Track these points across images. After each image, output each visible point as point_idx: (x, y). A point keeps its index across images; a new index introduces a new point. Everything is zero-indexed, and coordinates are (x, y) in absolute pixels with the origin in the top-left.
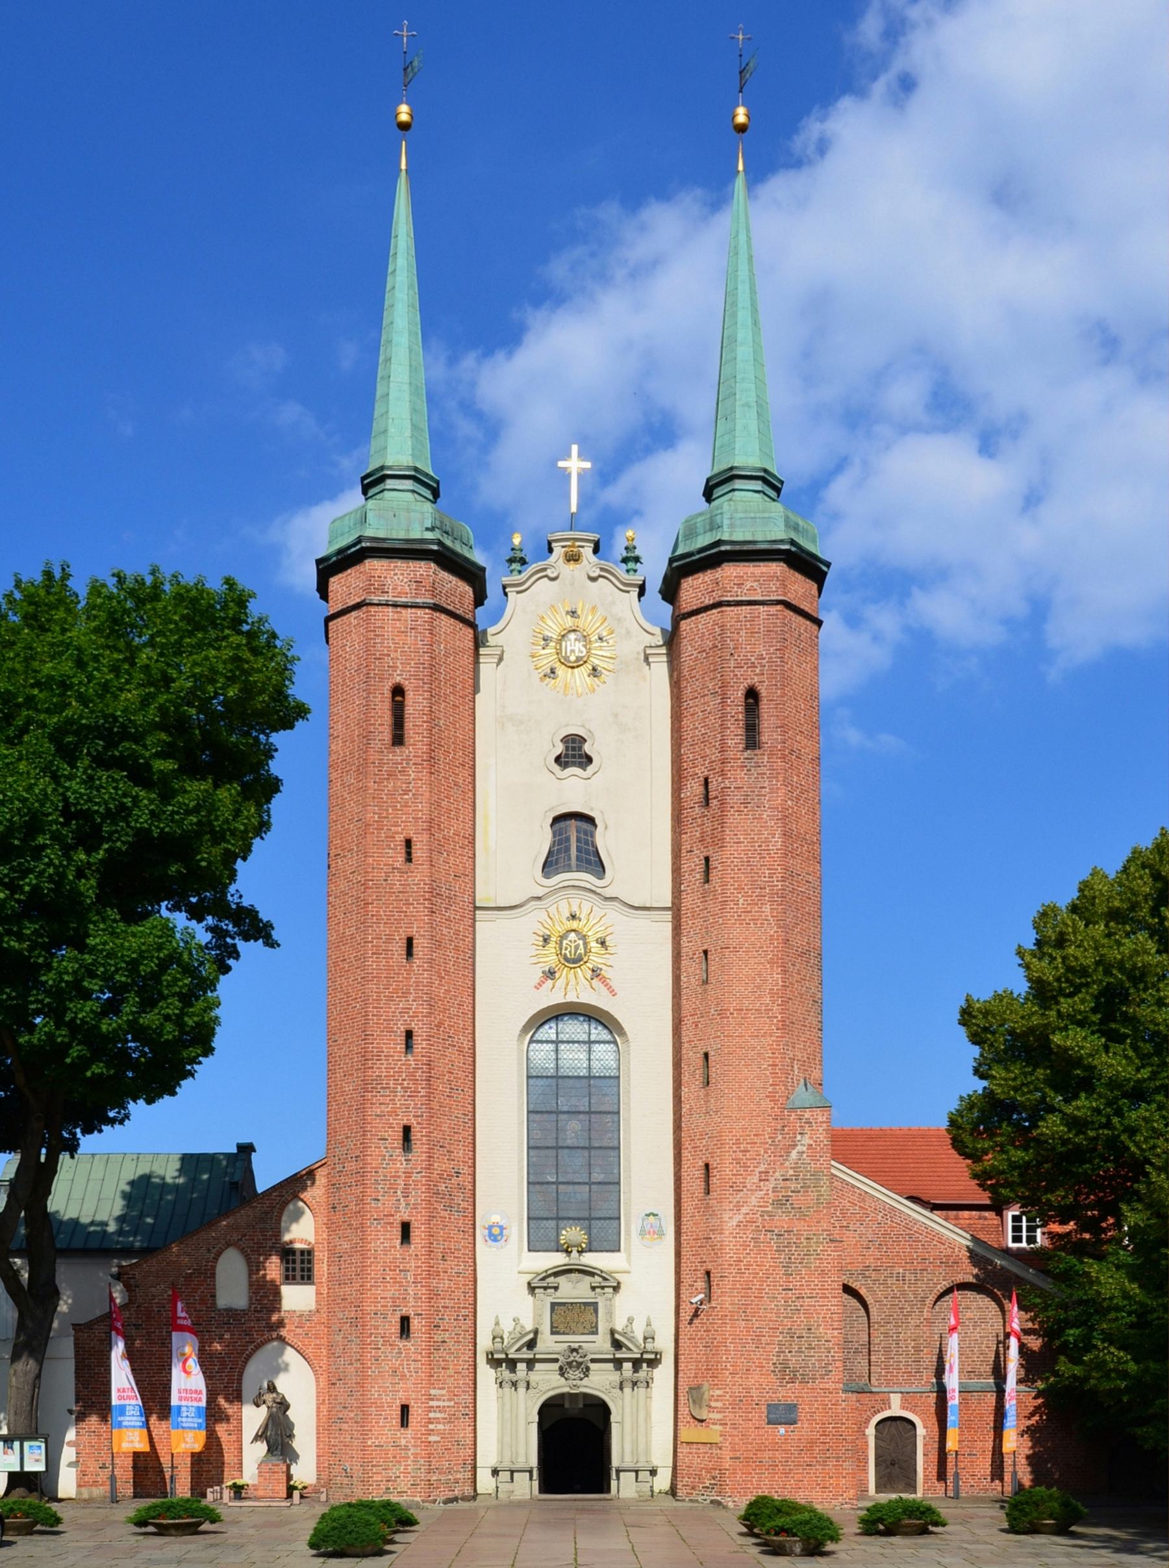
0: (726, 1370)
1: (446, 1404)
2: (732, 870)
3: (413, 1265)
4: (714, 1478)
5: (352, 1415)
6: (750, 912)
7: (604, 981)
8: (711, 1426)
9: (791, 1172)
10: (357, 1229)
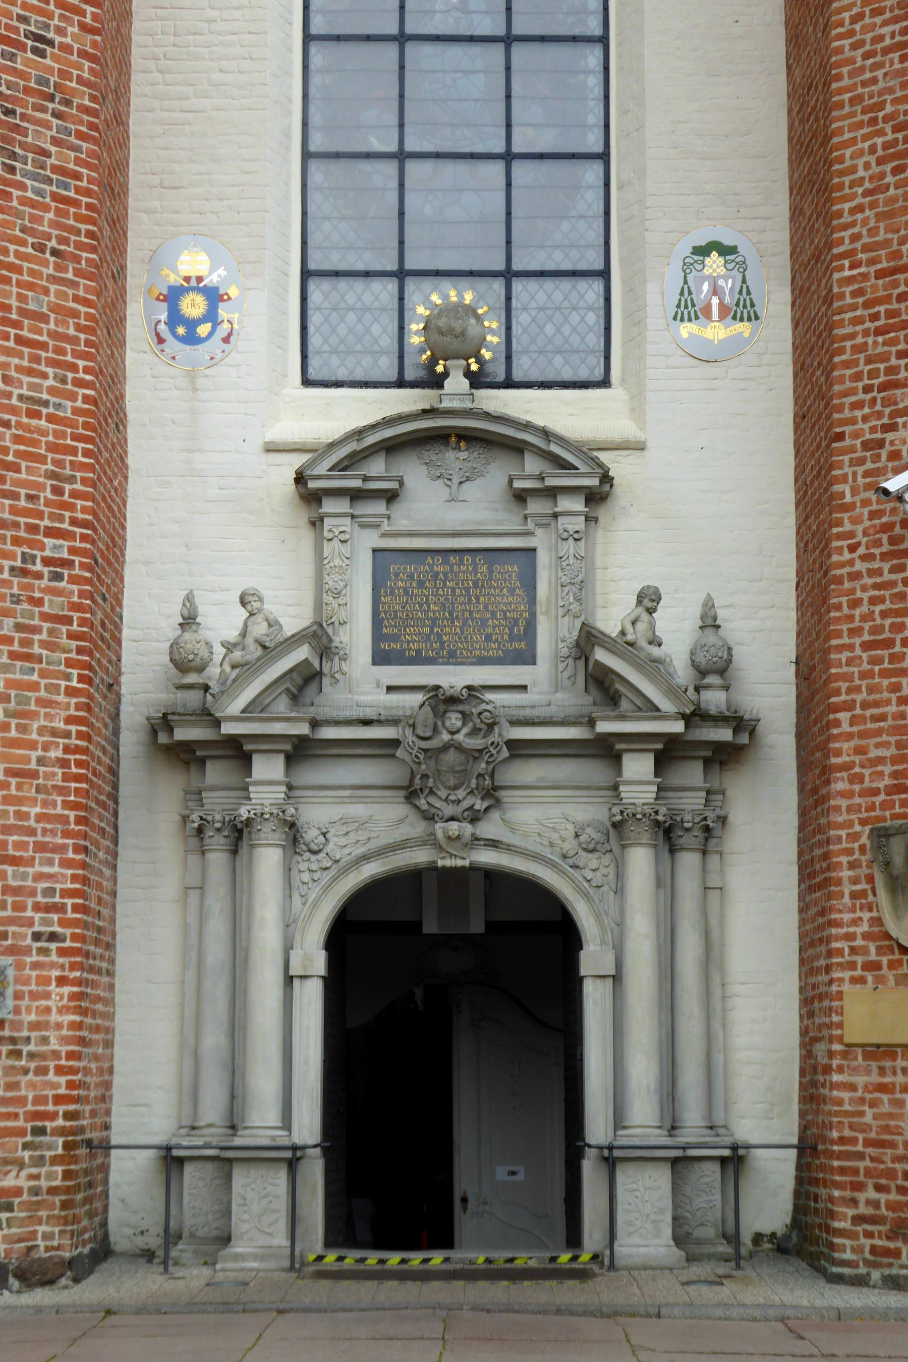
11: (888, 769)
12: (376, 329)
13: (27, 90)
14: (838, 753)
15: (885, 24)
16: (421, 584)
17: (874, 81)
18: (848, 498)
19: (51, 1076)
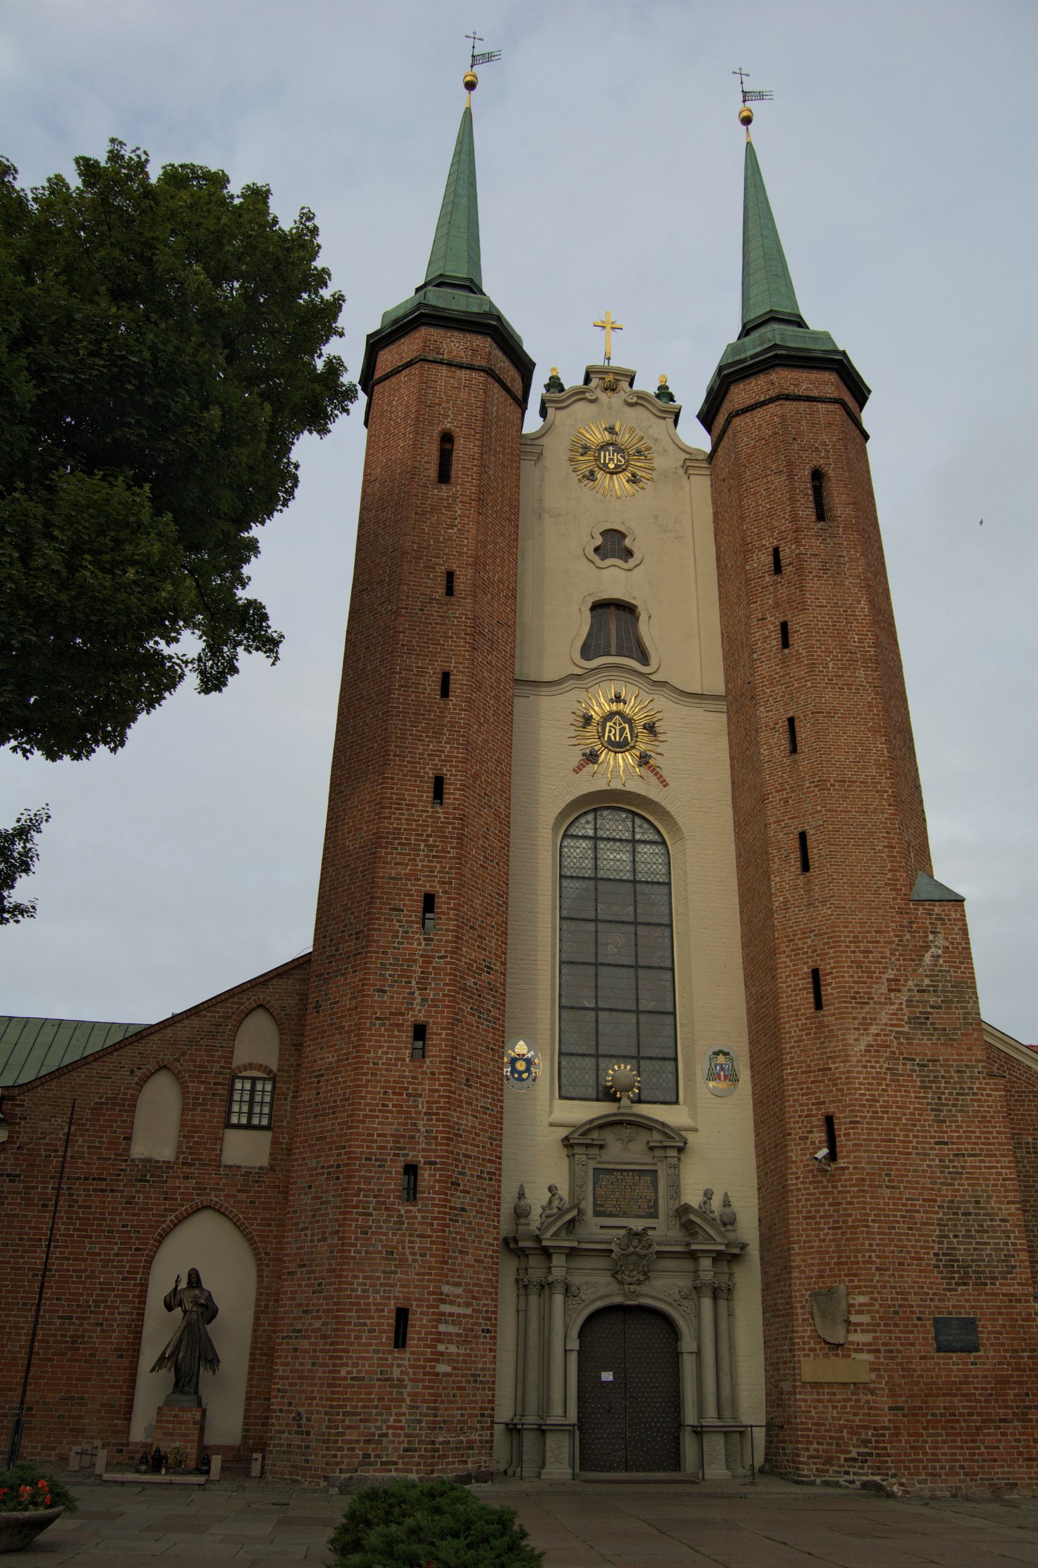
0: (872, 1263)
1: (462, 1310)
2: (817, 633)
3: (427, 1087)
4: (865, 1443)
5: (317, 1324)
6: (842, 676)
7: (655, 770)
8: (854, 1355)
9: (927, 981)
10: (349, 1032)
11: (816, 1268)
12: (587, 1077)
13: (485, 987)
14: (795, 1261)
15: (799, 979)
16: (612, 1183)
17: (796, 1000)
18: (794, 1159)
19: (487, 1392)
